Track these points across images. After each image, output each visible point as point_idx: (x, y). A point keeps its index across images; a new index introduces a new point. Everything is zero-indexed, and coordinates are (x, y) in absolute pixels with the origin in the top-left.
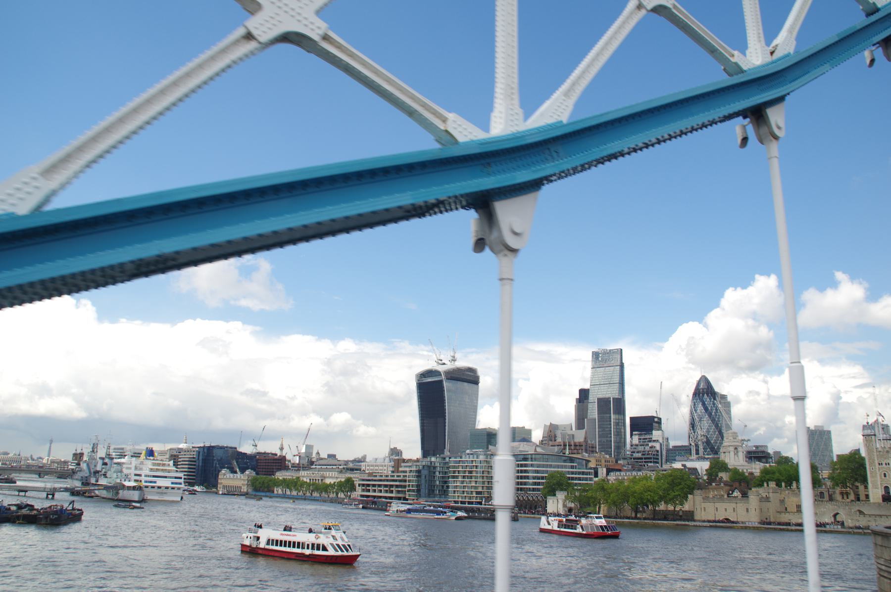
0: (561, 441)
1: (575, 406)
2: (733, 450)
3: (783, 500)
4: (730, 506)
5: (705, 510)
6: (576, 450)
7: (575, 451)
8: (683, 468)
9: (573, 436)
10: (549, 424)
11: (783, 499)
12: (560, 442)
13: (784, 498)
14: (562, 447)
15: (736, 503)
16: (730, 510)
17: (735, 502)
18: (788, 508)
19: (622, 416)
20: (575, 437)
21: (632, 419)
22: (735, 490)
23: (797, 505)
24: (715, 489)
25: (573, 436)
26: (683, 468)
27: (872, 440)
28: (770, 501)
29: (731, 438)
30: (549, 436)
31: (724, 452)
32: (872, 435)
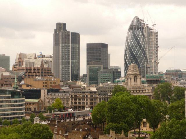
0: (24, 67)
1: (54, 34)
2: (133, 77)
6: (35, 73)
7: (34, 74)
8: (97, 90)
9: (33, 63)
12: (24, 68)
14: (25, 71)
19: (78, 45)
20: (35, 64)
21: (89, 46)
22: (89, 135)
24: (77, 133)
25: (33, 63)
26: (97, 90)
29: (133, 69)
30: (19, 62)
31: (128, 79)
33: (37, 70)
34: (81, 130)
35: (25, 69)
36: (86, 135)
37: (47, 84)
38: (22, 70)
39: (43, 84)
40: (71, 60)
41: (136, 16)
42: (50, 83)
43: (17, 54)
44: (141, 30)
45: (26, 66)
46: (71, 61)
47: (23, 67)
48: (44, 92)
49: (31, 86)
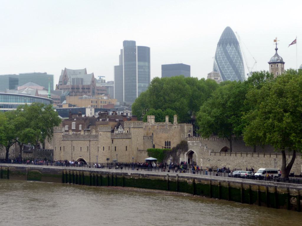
1: (120, 56)
3: (151, 136)
4: (84, 144)
5: (64, 150)
10: (64, 70)
11: (151, 135)
12: (68, 86)
13: (153, 134)
14: (70, 90)
15: (90, 141)
16: (85, 149)
17: (88, 139)
18: (155, 146)
22: (119, 125)
23: (166, 142)
25: (82, 80)
27: (278, 68)
28: (130, 138)
32: (278, 62)
33: (87, 88)
34: (108, 119)
35: (70, 87)
36: (115, 126)
37: (96, 104)
38: (66, 89)
39: (92, 104)
40: (138, 83)
41: (229, 26)
42: (101, 102)
43: (62, 70)
44: (234, 45)
45: (72, 84)
46: (139, 85)
47: (67, 84)
48: (90, 112)
49: (74, 106)
